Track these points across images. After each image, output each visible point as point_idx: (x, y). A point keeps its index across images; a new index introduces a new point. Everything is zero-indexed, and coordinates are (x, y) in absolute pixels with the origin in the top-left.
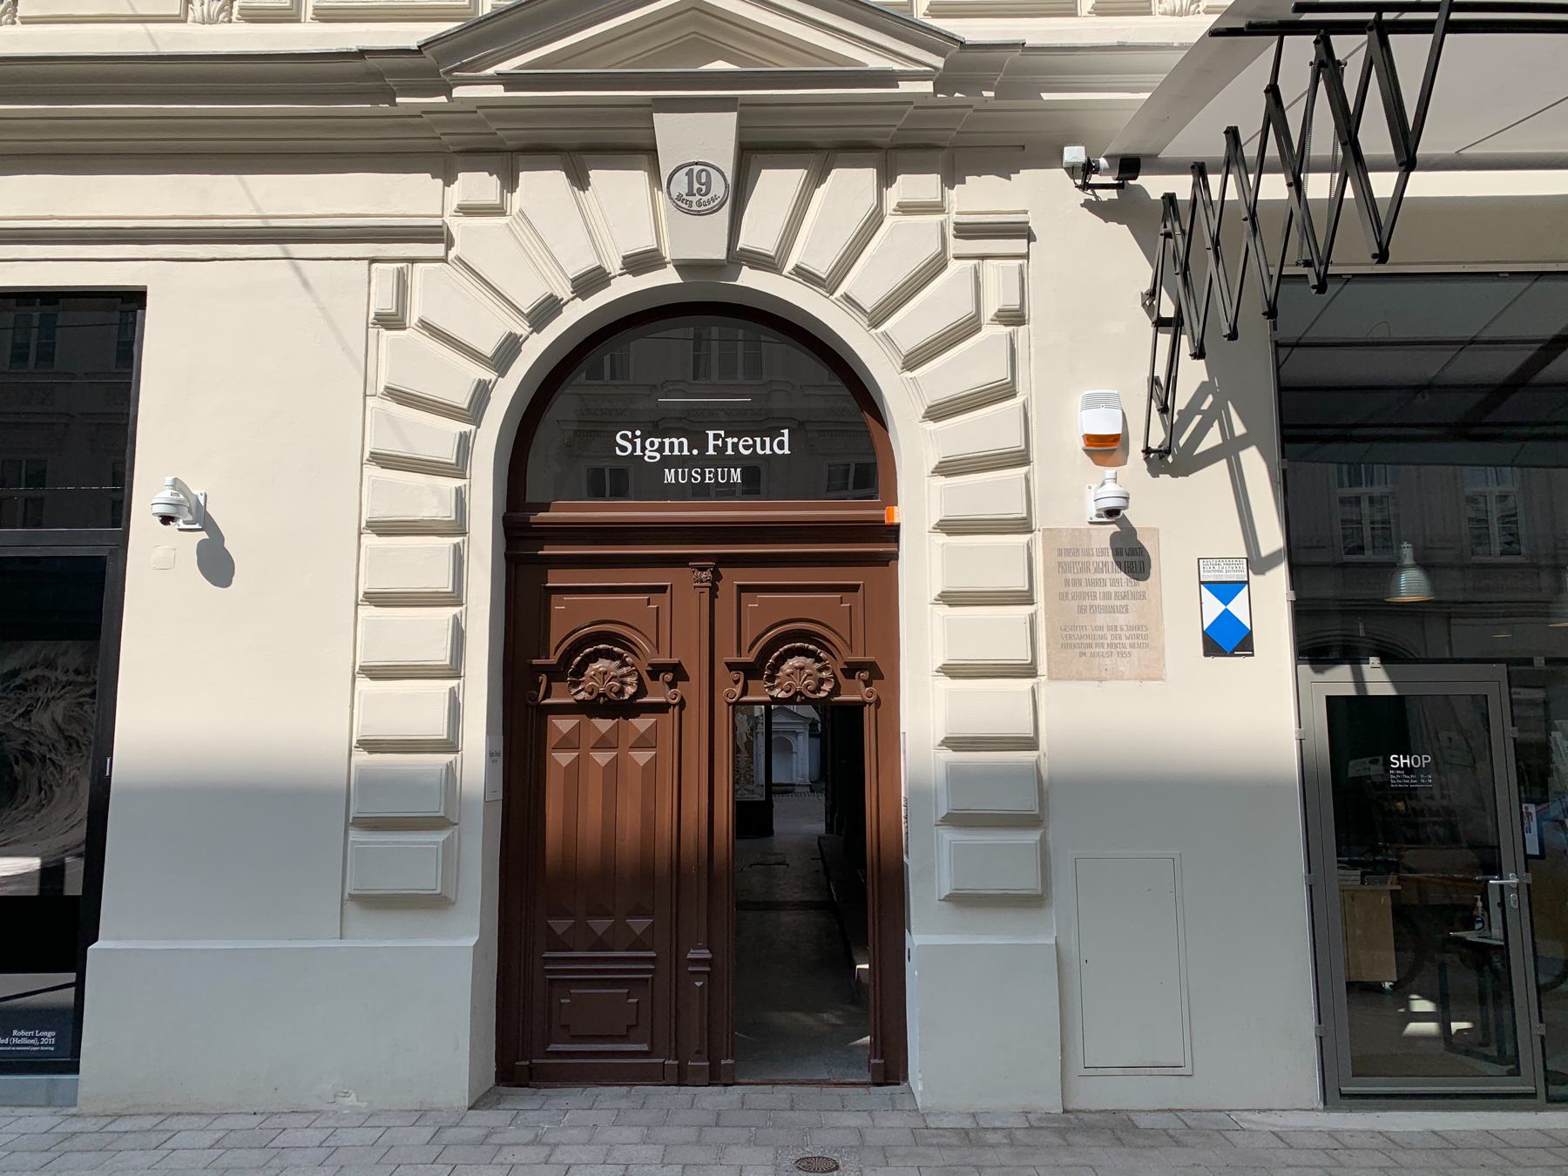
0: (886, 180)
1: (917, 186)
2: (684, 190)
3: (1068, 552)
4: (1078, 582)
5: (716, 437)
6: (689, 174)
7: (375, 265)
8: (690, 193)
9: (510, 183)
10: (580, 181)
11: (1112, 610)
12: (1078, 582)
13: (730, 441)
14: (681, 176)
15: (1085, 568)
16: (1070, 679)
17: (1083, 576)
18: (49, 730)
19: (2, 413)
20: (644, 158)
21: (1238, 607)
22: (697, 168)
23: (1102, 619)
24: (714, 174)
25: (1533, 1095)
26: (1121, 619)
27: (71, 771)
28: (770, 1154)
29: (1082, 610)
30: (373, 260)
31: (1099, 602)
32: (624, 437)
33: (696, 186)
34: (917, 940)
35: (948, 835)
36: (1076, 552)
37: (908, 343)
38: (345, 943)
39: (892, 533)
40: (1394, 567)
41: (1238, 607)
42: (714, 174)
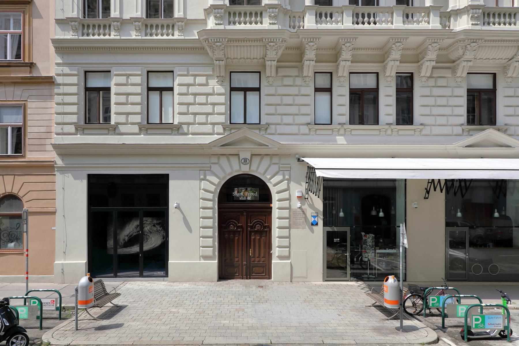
0: (271, 159)
1: (275, 160)
2: (243, 162)
3: (294, 212)
4: (295, 216)
5: (247, 193)
6: (244, 160)
7: (201, 171)
8: (244, 162)
9: (219, 159)
10: (228, 159)
11: (300, 219)
12: (295, 216)
13: (249, 194)
14: (243, 160)
15: (296, 214)
16: (294, 228)
17: (296, 215)
18: (147, 231)
19: (1, 83)
20: (237, 156)
21: (316, 219)
22: (245, 159)
23: (298, 221)
24: (248, 160)
25: (349, 280)
26: (301, 221)
27: (151, 237)
28: (255, 286)
29: (296, 219)
30: (200, 170)
31: (298, 218)
32: (234, 193)
33: (245, 161)
34: (273, 261)
35: (278, 249)
36: (295, 212)
37: (273, 183)
38: (201, 261)
39: (271, 208)
40: (340, 212)
41: (316, 219)
42: (248, 160)
